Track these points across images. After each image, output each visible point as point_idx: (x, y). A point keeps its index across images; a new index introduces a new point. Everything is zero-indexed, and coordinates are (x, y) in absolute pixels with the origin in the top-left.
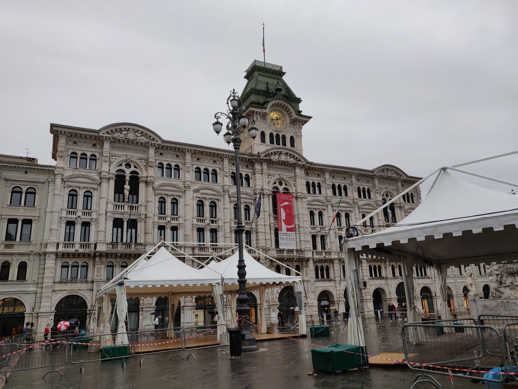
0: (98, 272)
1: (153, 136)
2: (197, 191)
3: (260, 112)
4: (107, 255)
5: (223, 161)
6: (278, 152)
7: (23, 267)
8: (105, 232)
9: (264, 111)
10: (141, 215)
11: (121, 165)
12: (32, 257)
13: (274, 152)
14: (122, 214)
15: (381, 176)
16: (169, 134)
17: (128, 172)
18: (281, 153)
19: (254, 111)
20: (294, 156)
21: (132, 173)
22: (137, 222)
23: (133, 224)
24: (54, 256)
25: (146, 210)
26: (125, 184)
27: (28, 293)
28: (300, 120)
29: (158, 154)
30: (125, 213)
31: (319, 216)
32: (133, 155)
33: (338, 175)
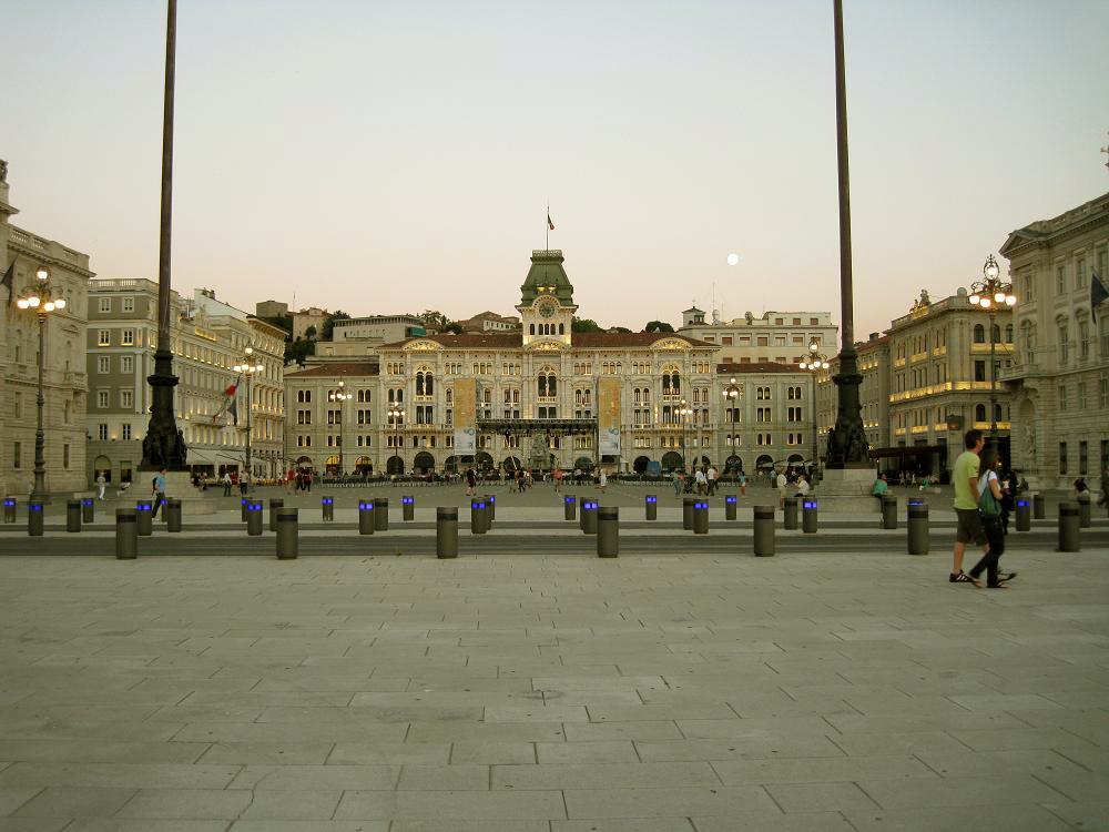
17: (425, 372)
23: (429, 409)
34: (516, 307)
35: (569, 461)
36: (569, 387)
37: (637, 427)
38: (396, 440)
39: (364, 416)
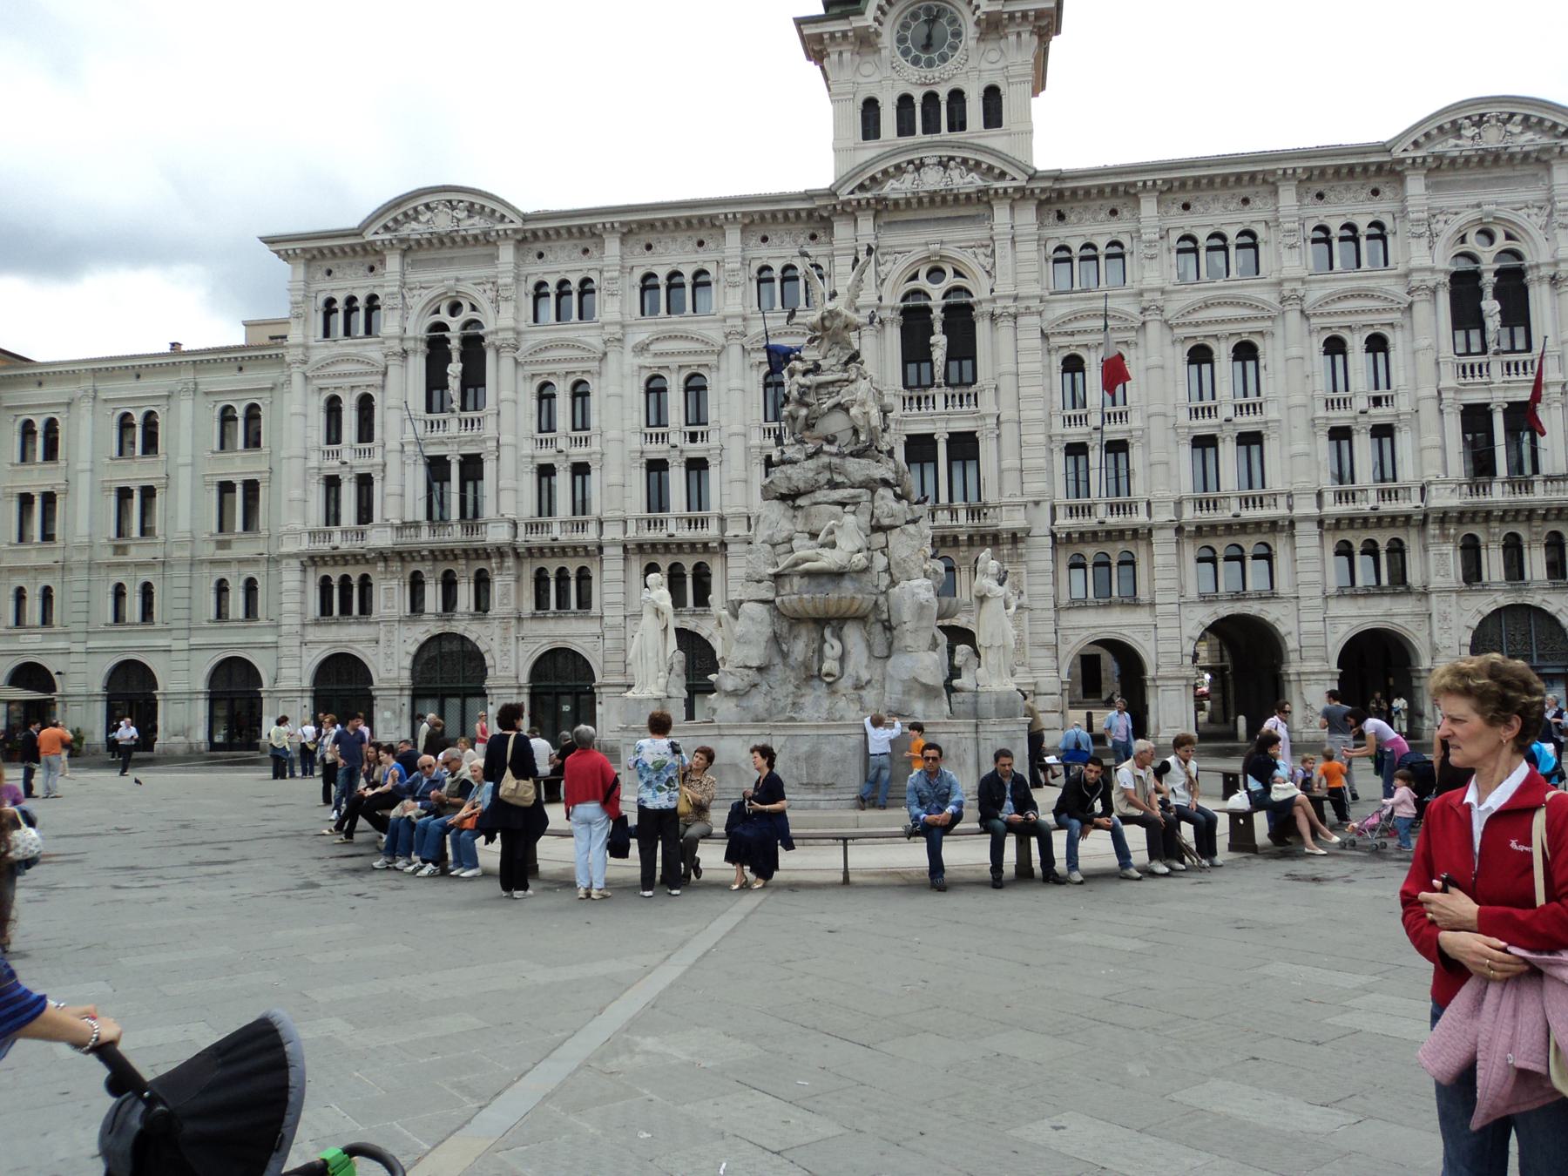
0: (387, 598)
1: (500, 210)
2: (642, 349)
3: (845, 34)
4: (401, 556)
5: (1276, 193)
6: (910, 162)
7: (251, 586)
8: (402, 495)
9: (858, 22)
10: (484, 441)
11: (437, 311)
12: (263, 568)
13: (898, 167)
14: (443, 443)
15: (1439, 158)
16: (532, 193)
17: (455, 325)
18: (920, 166)
19: (821, 35)
20: (978, 163)
21: (466, 325)
22: (481, 462)
23: (472, 467)
24: (295, 564)
25: (997, 403)
26: (450, 361)
27: (263, 647)
28: (1012, 16)
29: (532, 257)
30: (452, 440)
31: (574, 396)
32: (462, 274)
33: (1207, 195)
34: (800, 22)
35: (1044, 660)
36: (1032, 340)
37: (1340, 497)
38: (344, 595)
39: (242, 501)
